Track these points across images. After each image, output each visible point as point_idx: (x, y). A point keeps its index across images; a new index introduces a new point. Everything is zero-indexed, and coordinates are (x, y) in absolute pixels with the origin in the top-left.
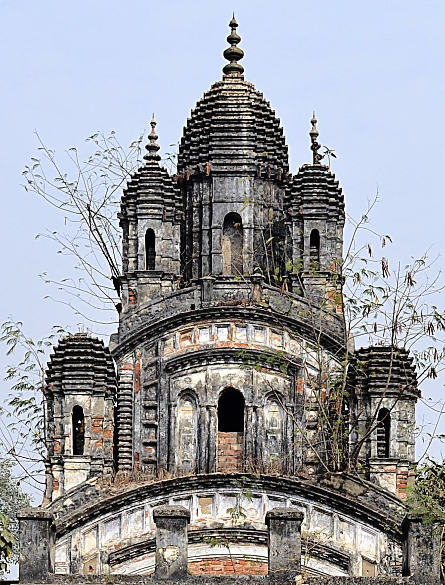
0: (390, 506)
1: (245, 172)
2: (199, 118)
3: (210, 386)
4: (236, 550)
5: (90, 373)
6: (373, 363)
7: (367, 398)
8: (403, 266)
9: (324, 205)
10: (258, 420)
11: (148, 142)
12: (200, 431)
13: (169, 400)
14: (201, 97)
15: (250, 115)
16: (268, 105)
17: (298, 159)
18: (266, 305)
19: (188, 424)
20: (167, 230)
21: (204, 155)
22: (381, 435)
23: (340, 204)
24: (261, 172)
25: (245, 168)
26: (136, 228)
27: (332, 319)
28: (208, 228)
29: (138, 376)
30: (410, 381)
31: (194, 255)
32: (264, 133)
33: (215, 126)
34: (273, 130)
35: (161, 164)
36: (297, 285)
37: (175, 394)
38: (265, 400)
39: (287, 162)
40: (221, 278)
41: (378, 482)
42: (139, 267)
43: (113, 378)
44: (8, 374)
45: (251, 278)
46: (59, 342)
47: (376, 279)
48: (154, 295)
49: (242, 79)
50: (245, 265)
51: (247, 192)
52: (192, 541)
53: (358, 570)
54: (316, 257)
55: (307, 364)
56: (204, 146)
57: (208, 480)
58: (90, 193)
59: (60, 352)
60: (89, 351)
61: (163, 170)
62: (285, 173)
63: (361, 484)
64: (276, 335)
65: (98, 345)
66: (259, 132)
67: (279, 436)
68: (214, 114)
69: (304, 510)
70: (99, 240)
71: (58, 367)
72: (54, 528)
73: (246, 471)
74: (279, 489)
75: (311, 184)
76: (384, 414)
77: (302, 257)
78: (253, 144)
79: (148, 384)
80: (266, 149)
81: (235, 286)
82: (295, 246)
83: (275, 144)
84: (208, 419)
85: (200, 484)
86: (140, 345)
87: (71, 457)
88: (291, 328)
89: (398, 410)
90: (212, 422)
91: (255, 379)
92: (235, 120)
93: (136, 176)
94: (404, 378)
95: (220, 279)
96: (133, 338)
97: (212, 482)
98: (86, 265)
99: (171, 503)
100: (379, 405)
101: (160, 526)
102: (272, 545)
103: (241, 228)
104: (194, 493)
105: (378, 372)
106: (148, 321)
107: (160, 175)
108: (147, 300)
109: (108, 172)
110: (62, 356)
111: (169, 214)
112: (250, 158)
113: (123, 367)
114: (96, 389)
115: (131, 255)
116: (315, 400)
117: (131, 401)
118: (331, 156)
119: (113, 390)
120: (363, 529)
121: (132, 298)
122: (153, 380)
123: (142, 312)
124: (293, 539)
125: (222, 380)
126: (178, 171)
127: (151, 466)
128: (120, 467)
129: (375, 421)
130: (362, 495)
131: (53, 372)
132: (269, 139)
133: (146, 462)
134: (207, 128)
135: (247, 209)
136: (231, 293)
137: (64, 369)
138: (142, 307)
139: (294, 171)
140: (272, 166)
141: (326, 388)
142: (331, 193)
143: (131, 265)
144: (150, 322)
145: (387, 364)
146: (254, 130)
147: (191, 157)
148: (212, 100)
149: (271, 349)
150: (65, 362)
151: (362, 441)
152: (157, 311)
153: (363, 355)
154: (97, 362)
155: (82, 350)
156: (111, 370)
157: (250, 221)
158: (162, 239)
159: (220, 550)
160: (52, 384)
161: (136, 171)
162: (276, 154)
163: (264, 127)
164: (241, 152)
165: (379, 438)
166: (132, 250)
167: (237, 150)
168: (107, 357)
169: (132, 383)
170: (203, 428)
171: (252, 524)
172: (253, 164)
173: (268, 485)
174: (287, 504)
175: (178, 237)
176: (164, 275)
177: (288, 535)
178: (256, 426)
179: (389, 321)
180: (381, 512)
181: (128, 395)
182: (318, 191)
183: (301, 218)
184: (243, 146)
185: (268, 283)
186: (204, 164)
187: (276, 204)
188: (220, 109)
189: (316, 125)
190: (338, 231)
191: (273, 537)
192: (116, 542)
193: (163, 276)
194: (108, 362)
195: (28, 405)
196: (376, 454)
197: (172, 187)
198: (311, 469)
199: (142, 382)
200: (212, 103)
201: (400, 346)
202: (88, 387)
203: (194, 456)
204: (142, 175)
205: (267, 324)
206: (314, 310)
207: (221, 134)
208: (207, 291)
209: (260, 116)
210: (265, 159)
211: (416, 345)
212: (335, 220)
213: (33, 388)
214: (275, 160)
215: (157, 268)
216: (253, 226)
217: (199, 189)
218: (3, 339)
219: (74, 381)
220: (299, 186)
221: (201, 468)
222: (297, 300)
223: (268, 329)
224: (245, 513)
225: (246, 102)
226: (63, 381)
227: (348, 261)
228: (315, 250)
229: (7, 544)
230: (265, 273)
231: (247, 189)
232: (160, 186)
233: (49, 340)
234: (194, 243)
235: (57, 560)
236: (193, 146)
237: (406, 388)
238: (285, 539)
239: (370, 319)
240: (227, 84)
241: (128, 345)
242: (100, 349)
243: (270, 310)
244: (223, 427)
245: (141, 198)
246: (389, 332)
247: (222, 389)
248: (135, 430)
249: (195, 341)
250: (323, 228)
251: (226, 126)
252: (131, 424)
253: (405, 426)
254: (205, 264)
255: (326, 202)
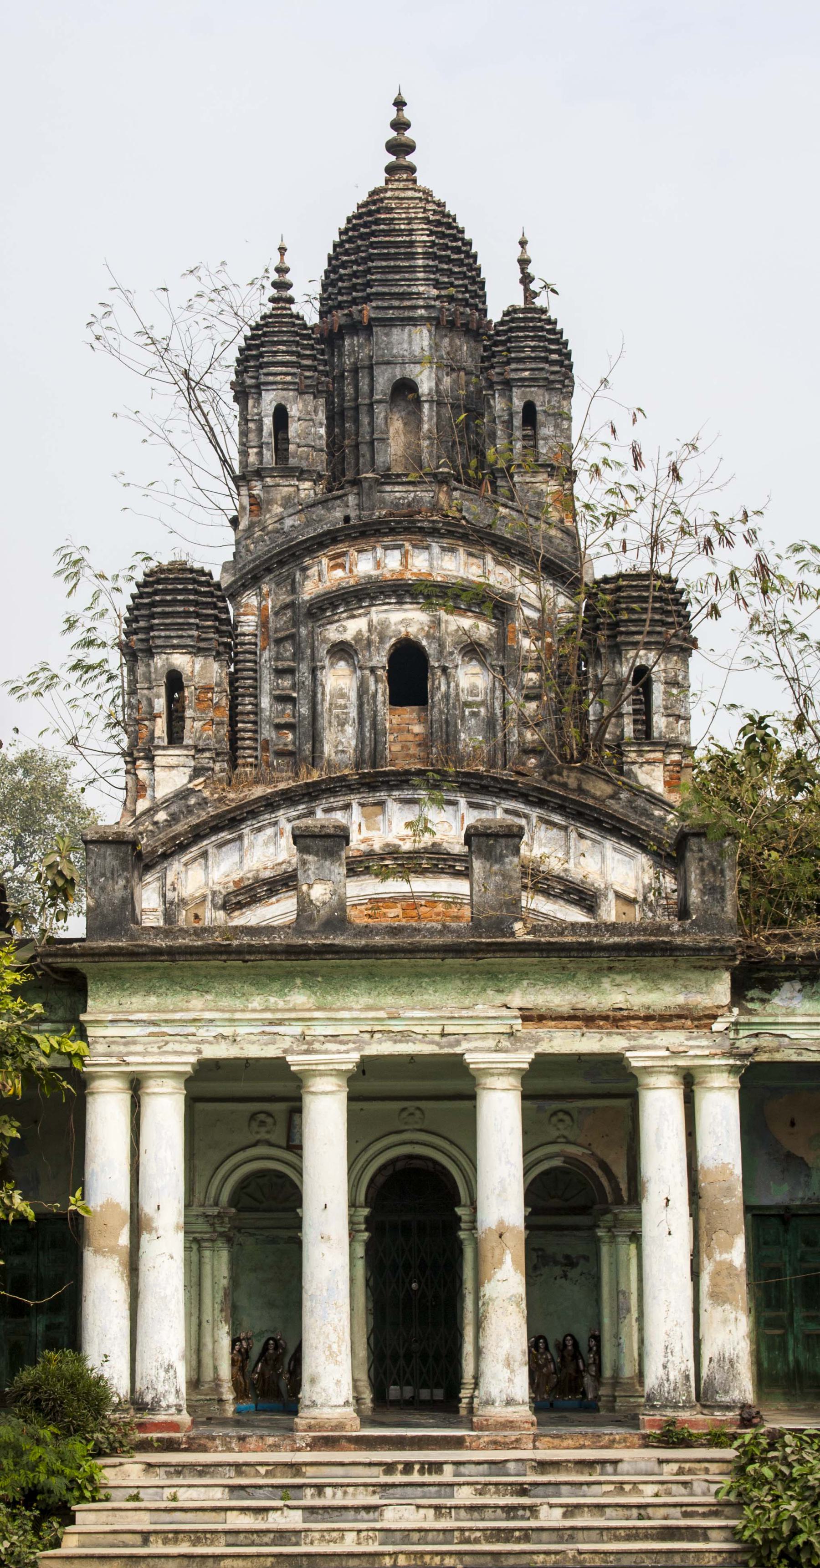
0: (656, 813)
1: (422, 318)
2: (350, 240)
3: (375, 637)
4: (421, 885)
5: (192, 621)
6: (623, 597)
7: (617, 651)
8: (664, 454)
9: (541, 366)
10: (449, 687)
11: (274, 276)
12: (360, 706)
13: (313, 658)
14: (352, 210)
15: (428, 235)
16: (454, 220)
17: (501, 297)
18: (457, 515)
19: (342, 695)
20: (305, 405)
21: (360, 294)
22: (638, 707)
23: (566, 362)
24: (446, 317)
25: (421, 312)
26: (259, 403)
27: (559, 535)
28: (367, 401)
29: (264, 623)
30: (680, 624)
31: (346, 442)
32: (449, 261)
33: (375, 251)
34: (462, 256)
35: (295, 308)
36: (504, 484)
37: (323, 651)
38: (458, 659)
39: (484, 303)
40: (388, 476)
41: (636, 777)
42: (265, 460)
43: (228, 629)
44: (66, 626)
45: (435, 475)
46: (145, 575)
47: (624, 473)
48: (287, 502)
49: (414, 181)
50: (425, 456)
51: (426, 348)
52: (352, 872)
53: (610, 912)
54: (531, 443)
55: (522, 601)
56: (359, 281)
57: (375, 779)
58: (188, 352)
59: (146, 590)
60: (190, 587)
61: (298, 317)
62: (481, 319)
63: (609, 780)
64: (475, 560)
65: (203, 579)
66: (441, 259)
67: (483, 710)
68: (373, 234)
69: (523, 822)
70: (203, 421)
71: (144, 612)
72: (139, 856)
73: (432, 765)
74: (484, 790)
75: (521, 334)
76: (642, 675)
77: (511, 443)
78: (432, 276)
79: (279, 635)
80: (452, 285)
81: (411, 489)
82: (499, 427)
83: (465, 277)
84: (372, 688)
85: (363, 785)
86: (268, 578)
87: (164, 748)
88: (498, 549)
89: (663, 667)
90: (380, 691)
91: (443, 625)
92: (405, 242)
93: (258, 327)
94: (670, 620)
95: (388, 477)
96: (257, 567)
97: (382, 782)
98: (184, 460)
99: (319, 814)
100: (634, 661)
101: (303, 850)
102: (476, 876)
103: (418, 402)
104: (354, 800)
105: (631, 611)
106: (280, 541)
107: (294, 325)
108: (277, 509)
109: (215, 321)
110: (149, 595)
111: (308, 382)
112: (429, 298)
113: (242, 610)
114: (202, 645)
115: (252, 444)
116: (535, 655)
117: (255, 662)
118: (550, 293)
119: (227, 645)
120: (615, 849)
121: (253, 508)
122: (288, 629)
123: (270, 528)
124: (508, 867)
125: (393, 627)
126: (321, 318)
127: (287, 759)
128: (240, 761)
129: (629, 686)
130: (612, 797)
131: (136, 620)
132: (456, 270)
133: (279, 754)
134: (363, 255)
135: (426, 372)
136: (404, 498)
137: (152, 616)
138: (269, 521)
139: (495, 315)
140: (462, 309)
141: (552, 637)
142: (553, 347)
143: (252, 459)
144: (283, 544)
145: (645, 600)
146: (434, 257)
147: (340, 298)
148: (370, 213)
149: (467, 580)
150: (153, 604)
151: (610, 716)
152: (293, 526)
153: (607, 586)
154: (203, 603)
155: (180, 587)
156: (224, 616)
157: (431, 390)
158: (299, 419)
159: (395, 886)
160: (135, 637)
161: (258, 319)
162: (467, 291)
163: (449, 252)
164: (414, 289)
165: (636, 712)
166: (252, 436)
167: (409, 286)
168: (217, 597)
169: (256, 635)
170: (365, 700)
171: (445, 845)
172: (433, 307)
173: (467, 784)
174: (498, 813)
175: (321, 416)
176: (302, 472)
177: (500, 859)
178: (447, 696)
179: (646, 535)
180: (641, 823)
181: (250, 653)
182: (532, 344)
183: (508, 385)
184: (418, 280)
185: (459, 481)
186: (360, 308)
187: (469, 364)
188: (382, 227)
189: (528, 247)
190: (565, 403)
191: (477, 865)
192: (236, 877)
193: (301, 474)
194: (220, 604)
195: (97, 671)
196: (632, 735)
197: (312, 342)
198: (533, 760)
199: (271, 634)
200: (370, 219)
201: (664, 571)
202: (189, 642)
203: (353, 743)
204: (267, 325)
205: (460, 543)
206: (531, 521)
207: (384, 264)
208: (368, 495)
209: (443, 236)
210: (451, 299)
211: (690, 570)
212: (559, 386)
213: (104, 644)
214: (466, 300)
215: (293, 462)
216: (435, 398)
217: (352, 345)
218: (59, 573)
219: (168, 633)
220: (503, 338)
221: (363, 762)
222: (505, 506)
223: (461, 550)
224: (434, 829)
225: (421, 215)
226: (152, 634)
227: (581, 446)
228: (530, 433)
229: (66, 880)
230: (454, 468)
231: (426, 343)
232: (293, 341)
233: (130, 573)
234: (347, 425)
235: (145, 905)
236: (343, 281)
237: (675, 635)
238: (496, 867)
239: (616, 533)
240: (392, 190)
241: (249, 576)
242: (207, 584)
243: (463, 522)
244: (397, 699)
245: (265, 360)
246: (645, 552)
247: (393, 640)
248: (263, 705)
249: (351, 571)
250: (542, 400)
251: (392, 251)
252: (256, 697)
253: (675, 691)
254: (364, 456)
255: (546, 360)
